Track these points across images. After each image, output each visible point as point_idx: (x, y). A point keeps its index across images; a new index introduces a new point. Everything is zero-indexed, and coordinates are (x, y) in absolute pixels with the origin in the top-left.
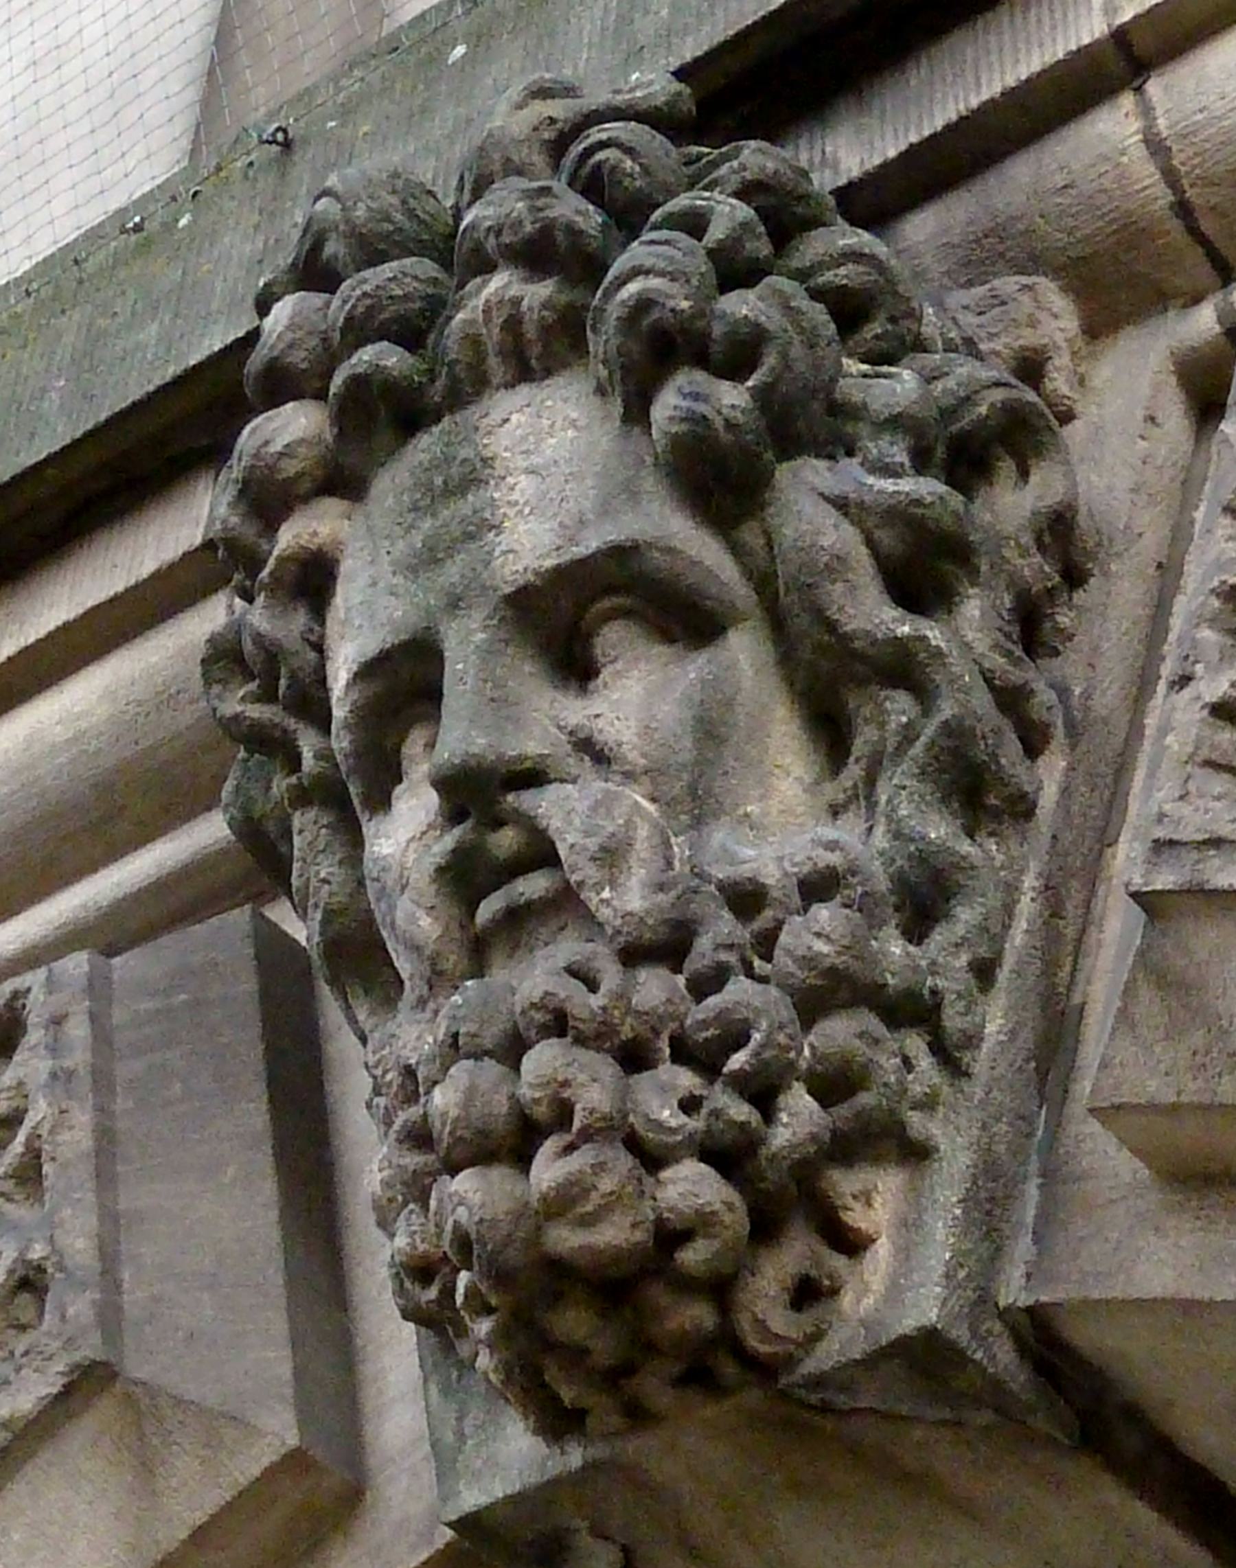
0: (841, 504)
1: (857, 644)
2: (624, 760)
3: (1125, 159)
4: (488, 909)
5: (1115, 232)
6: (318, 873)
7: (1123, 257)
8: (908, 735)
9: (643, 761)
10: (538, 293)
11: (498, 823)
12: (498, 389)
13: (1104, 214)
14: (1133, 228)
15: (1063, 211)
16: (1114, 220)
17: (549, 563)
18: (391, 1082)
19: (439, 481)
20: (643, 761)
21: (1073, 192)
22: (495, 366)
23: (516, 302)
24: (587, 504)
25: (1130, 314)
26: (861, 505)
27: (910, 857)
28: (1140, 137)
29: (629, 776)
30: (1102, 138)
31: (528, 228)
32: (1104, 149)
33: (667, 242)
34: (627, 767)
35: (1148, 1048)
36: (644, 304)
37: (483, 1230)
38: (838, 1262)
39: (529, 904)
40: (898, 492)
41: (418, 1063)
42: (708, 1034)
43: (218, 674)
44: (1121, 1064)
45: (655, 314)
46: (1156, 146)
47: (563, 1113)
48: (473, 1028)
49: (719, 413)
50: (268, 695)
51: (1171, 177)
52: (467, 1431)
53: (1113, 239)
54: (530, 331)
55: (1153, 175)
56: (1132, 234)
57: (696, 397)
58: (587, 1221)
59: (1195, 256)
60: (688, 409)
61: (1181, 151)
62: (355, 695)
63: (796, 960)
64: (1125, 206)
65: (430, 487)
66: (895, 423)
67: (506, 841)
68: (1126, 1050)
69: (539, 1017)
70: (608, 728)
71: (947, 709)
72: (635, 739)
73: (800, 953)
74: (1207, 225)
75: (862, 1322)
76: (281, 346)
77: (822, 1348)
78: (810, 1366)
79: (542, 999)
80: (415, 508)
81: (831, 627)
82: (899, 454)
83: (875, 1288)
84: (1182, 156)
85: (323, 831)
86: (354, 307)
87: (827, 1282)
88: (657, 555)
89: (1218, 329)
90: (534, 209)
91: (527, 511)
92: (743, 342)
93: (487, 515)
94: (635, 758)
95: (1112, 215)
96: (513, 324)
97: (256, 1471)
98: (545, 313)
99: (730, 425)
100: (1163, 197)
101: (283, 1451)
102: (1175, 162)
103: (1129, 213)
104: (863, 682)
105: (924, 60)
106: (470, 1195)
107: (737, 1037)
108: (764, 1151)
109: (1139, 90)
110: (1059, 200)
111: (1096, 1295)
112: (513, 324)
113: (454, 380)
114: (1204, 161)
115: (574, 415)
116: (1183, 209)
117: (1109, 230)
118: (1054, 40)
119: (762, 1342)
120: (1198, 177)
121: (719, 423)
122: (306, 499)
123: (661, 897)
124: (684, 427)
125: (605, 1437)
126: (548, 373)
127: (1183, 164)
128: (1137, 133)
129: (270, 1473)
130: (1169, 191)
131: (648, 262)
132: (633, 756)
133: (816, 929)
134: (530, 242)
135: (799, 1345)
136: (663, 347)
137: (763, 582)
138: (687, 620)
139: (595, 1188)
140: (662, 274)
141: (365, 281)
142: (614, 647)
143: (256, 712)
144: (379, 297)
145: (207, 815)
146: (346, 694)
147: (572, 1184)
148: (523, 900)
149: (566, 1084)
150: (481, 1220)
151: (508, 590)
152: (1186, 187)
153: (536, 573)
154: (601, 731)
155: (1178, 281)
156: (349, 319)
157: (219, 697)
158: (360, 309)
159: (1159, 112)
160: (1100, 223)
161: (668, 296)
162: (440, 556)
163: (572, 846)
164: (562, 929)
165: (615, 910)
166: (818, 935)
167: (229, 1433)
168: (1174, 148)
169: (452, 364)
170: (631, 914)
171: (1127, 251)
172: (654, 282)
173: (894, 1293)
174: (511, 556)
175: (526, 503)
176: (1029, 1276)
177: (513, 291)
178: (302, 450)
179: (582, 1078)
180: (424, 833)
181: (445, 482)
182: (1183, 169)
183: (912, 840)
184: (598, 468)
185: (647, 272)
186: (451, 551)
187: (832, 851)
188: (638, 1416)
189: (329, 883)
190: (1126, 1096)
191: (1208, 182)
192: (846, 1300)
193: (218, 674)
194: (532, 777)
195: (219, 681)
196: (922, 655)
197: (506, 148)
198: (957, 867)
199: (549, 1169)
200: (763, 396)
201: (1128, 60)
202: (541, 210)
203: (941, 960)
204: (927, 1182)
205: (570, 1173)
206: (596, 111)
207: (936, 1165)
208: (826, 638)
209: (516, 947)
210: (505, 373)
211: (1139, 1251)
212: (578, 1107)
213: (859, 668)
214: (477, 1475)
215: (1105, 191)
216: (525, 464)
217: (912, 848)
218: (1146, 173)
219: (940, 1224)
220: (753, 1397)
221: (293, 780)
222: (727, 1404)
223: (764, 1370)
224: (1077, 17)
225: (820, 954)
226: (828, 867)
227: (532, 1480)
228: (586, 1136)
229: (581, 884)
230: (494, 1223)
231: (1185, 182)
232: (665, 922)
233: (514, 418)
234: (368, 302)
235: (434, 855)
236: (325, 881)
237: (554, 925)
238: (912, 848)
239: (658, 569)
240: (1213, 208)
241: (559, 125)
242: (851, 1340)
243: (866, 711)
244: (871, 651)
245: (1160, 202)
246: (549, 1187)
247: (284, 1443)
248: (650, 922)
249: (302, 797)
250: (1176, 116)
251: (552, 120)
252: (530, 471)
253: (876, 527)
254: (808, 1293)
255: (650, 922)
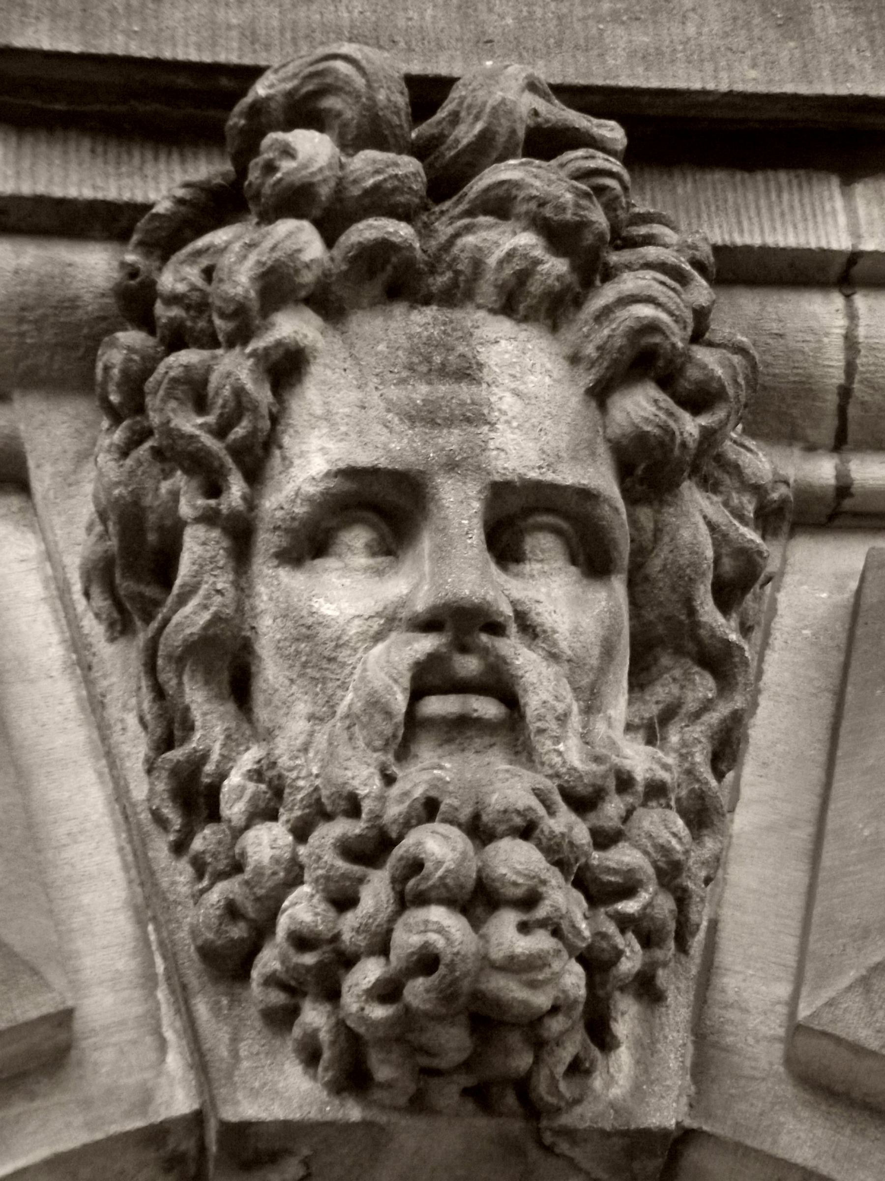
0: (712, 527)
1: (702, 632)
2: (555, 644)
3: (826, 340)
4: (436, 706)
5: (794, 382)
6: (214, 583)
7: (789, 400)
8: (706, 706)
9: (569, 652)
10: (555, 267)
11: (464, 649)
12: (479, 307)
13: (795, 368)
14: (807, 386)
15: (769, 350)
16: (797, 374)
17: (533, 475)
18: (302, 788)
19: (437, 359)
20: (569, 652)
21: (782, 341)
22: (486, 290)
23: (537, 262)
24: (563, 445)
25: (767, 435)
26: (725, 536)
27: (692, 791)
28: (843, 332)
29: (554, 657)
30: (814, 316)
31: (568, 216)
32: (813, 323)
33: (674, 290)
34: (554, 650)
35: (872, 1010)
36: (652, 327)
37: (457, 959)
38: (596, 1052)
39: (479, 720)
40: (752, 541)
41: (367, 796)
42: (613, 879)
43: (179, 394)
44: (845, 1010)
45: (657, 339)
46: (851, 343)
47: (529, 901)
48: (456, 803)
49: (682, 434)
50: (221, 431)
51: (850, 369)
52: (243, 1053)
53: (789, 386)
54: (535, 287)
55: (838, 361)
56: (805, 389)
57: (671, 414)
58: (533, 985)
59: (830, 424)
60: (665, 422)
61: (866, 356)
62: (332, 483)
63: (655, 846)
64: (812, 370)
65: (428, 360)
66: (758, 490)
67: (469, 665)
68: (854, 1002)
69: (518, 821)
70: (546, 614)
71: (739, 702)
72: (568, 634)
73: (661, 841)
74: (853, 411)
75: (612, 1105)
76: (319, 177)
77: (578, 1110)
78: (567, 1120)
79: (525, 810)
80: (411, 368)
81: (692, 612)
82: (750, 510)
83: (621, 1082)
84: (864, 360)
85: (221, 552)
86: (385, 180)
87: (587, 1065)
88: (607, 508)
89: (832, 481)
90: (577, 205)
91: (515, 424)
92: (708, 393)
93: (486, 411)
94: (564, 645)
95: (800, 371)
96: (523, 276)
97: (34, 1014)
98: (557, 284)
99: (684, 445)
100: (838, 377)
101: (61, 1007)
102: (858, 361)
103: (810, 376)
104: (679, 651)
105: (689, 180)
106: (453, 930)
107: (628, 891)
108: (614, 971)
109: (848, 297)
110: (770, 341)
111: (749, 1142)
112: (523, 276)
113: (455, 284)
114: (876, 371)
115: (549, 366)
116: (845, 392)
117: (792, 379)
118: (806, 229)
119: (548, 1093)
120: (866, 379)
121: (678, 440)
122: (297, 302)
123: (594, 767)
124: (656, 431)
125: (383, 1107)
126: (525, 319)
127: (862, 365)
128: (841, 327)
129: (44, 1019)
130: (843, 376)
131: (663, 299)
132: (564, 645)
133: (675, 830)
134: (565, 225)
135: (567, 1103)
136: (643, 360)
137: (641, 554)
138: (592, 558)
139: (550, 965)
140: (671, 313)
141: (396, 164)
142: (543, 551)
143: (209, 441)
144: (403, 182)
145: (318, 562)
146: (322, 480)
147: (540, 957)
148: (475, 715)
149: (544, 882)
150: (458, 953)
151: (497, 478)
152: (856, 380)
153: (520, 477)
154: (538, 614)
155: (809, 432)
156: (377, 187)
157: (174, 410)
158: (389, 185)
159: (862, 322)
160: (789, 372)
161: (673, 333)
162: (439, 421)
163: (545, 702)
164: (491, 746)
165: (564, 762)
166: (675, 835)
167: (26, 980)
168: (863, 352)
169: (457, 273)
170: (575, 769)
171: (794, 397)
172: (664, 316)
173: (637, 1090)
174: (503, 455)
175: (514, 418)
176: (691, 1106)
177: (538, 253)
178: (314, 267)
179: (554, 882)
180: (371, 617)
181: (443, 364)
182: (861, 369)
183: (698, 781)
184: (569, 420)
185: (657, 304)
186: (450, 422)
187: (666, 770)
188: (418, 1104)
189: (223, 595)
190: (838, 1030)
191: (870, 384)
192: (597, 1083)
193: (179, 394)
194: (496, 628)
195: (177, 399)
196: (737, 659)
197: (515, 121)
198: (716, 809)
199: (506, 934)
200: (709, 436)
201: (847, 274)
202: (584, 209)
203: (693, 870)
204: (657, 1021)
205: (542, 950)
206: (577, 129)
207: (664, 1009)
208: (683, 617)
209: (449, 741)
210: (496, 301)
211: (782, 1124)
212: (547, 902)
213: (690, 646)
214: (255, 1094)
215: (803, 353)
216: (513, 386)
217: (697, 786)
218: (835, 357)
219: (672, 1056)
220: (516, 1126)
221: (212, 502)
222: (494, 1122)
223: (533, 1110)
224: (825, 223)
225: (674, 849)
226: (662, 781)
227: (312, 1115)
228: (543, 924)
229: (541, 731)
230: (464, 959)
231: (857, 378)
232: (593, 785)
233: (503, 343)
234: (396, 183)
235: (416, 651)
236: (219, 592)
237: (487, 740)
238: (697, 786)
239: (603, 518)
240: (862, 403)
241: (540, 120)
242: (602, 1114)
243: (677, 673)
244: (707, 641)
245: (834, 381)
246: (523, 954)
247: (64, 1003)
248: (586, 781)
249: (209, 518)
250: (873, 332)
251: (536, 113)
252: (517, 393)
253: (727, 555)
254: (578, 1069)
255: (586, 781)
